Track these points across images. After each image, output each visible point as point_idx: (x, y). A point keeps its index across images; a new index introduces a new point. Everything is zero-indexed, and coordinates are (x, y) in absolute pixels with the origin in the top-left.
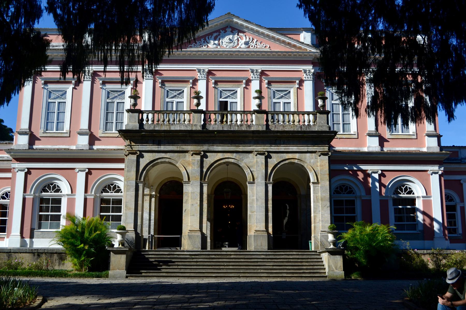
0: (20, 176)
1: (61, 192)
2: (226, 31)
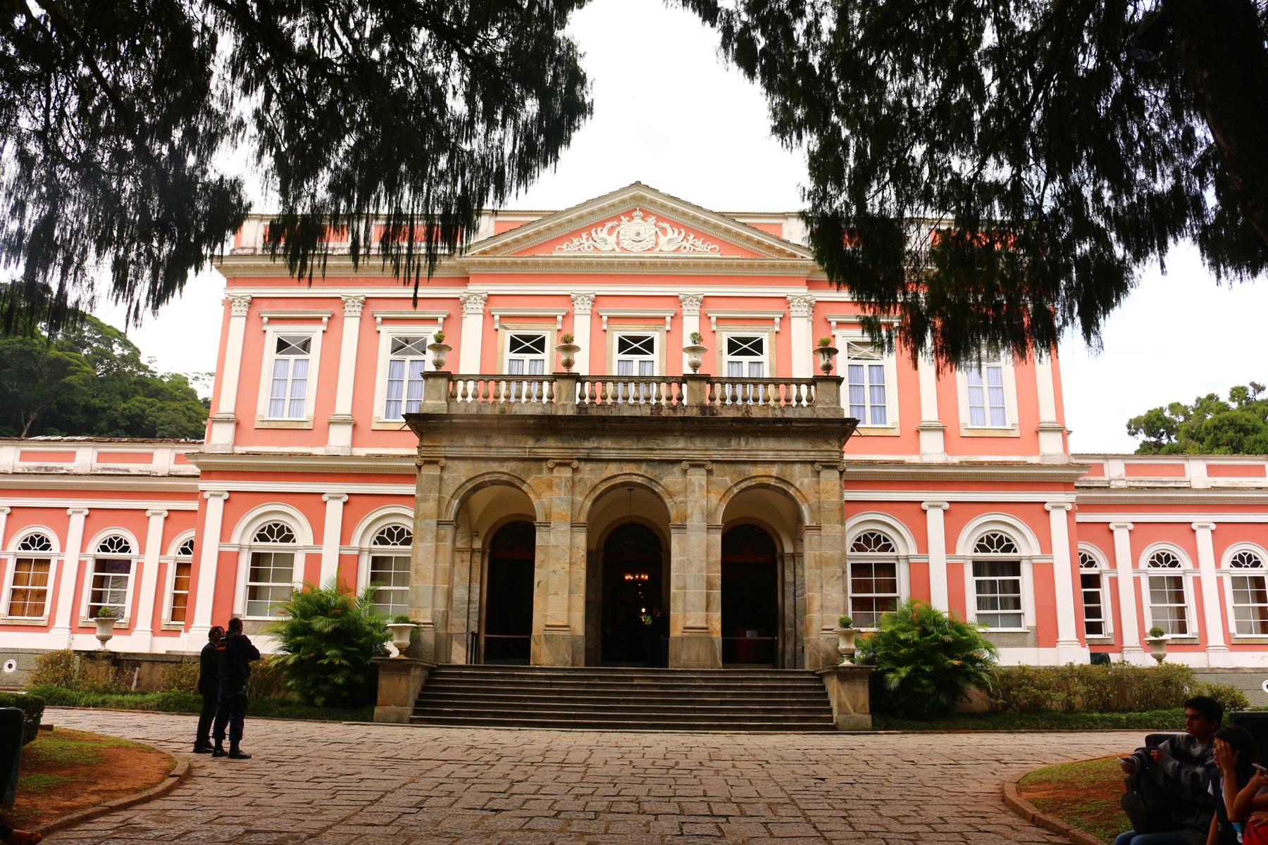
0: (215, 509)
1: (294, 541)
2: (632, 218)
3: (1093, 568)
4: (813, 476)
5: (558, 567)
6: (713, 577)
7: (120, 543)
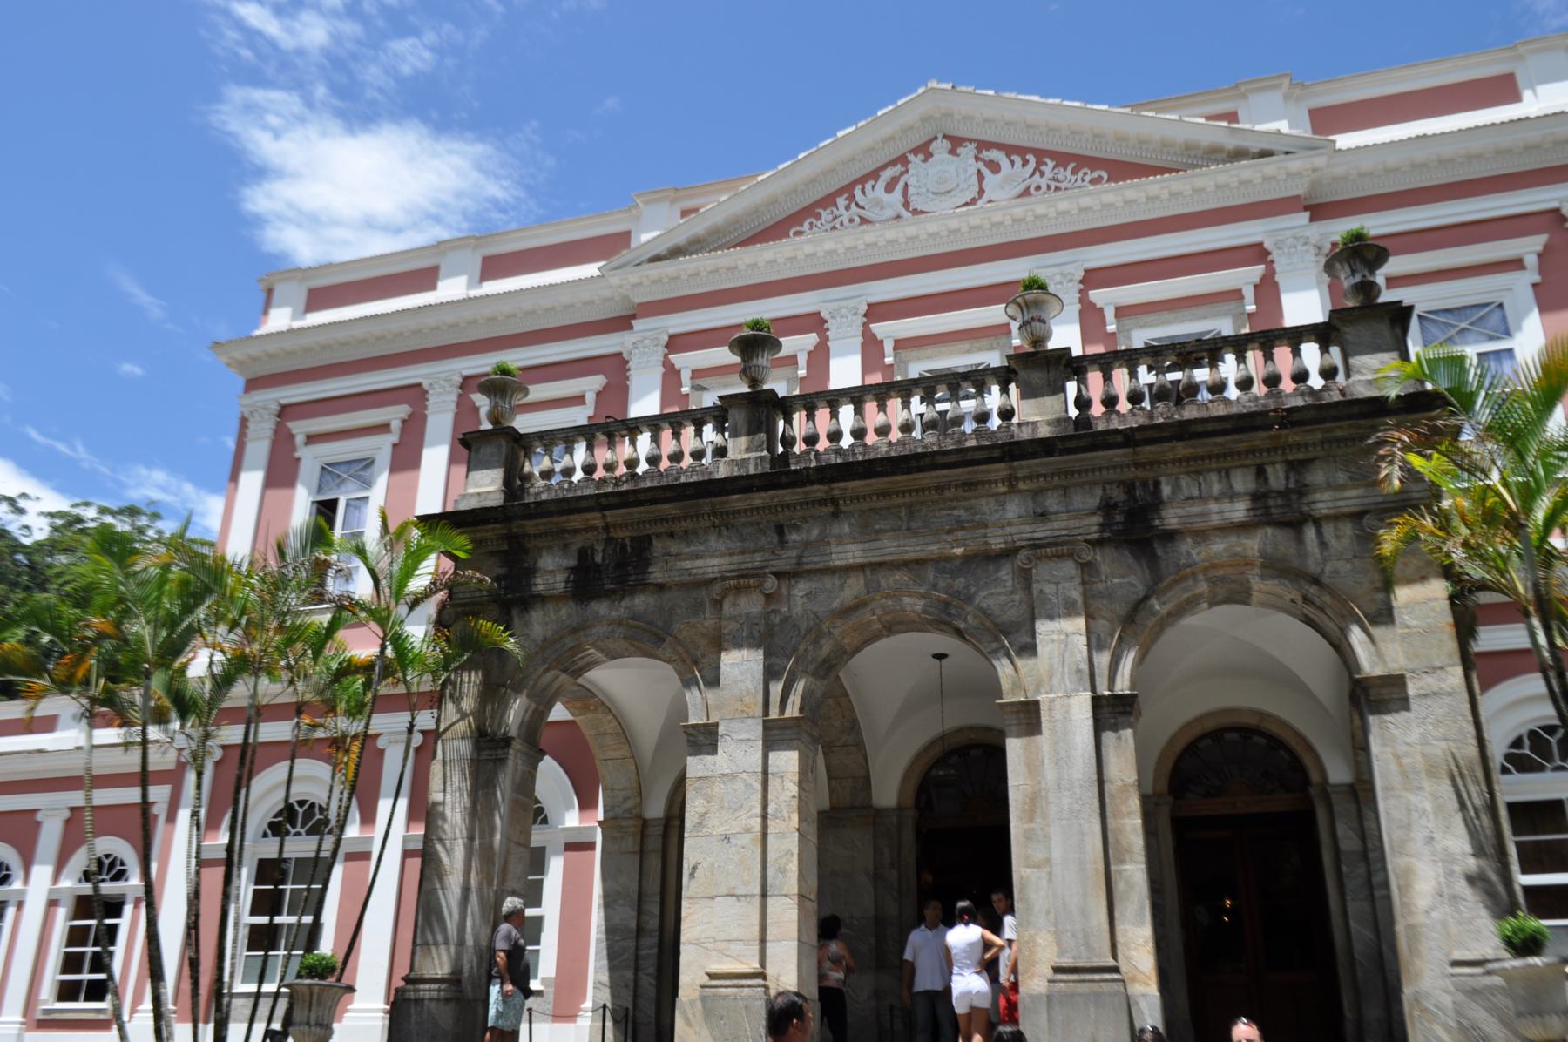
2: (928, 156)
7: (112, 865)
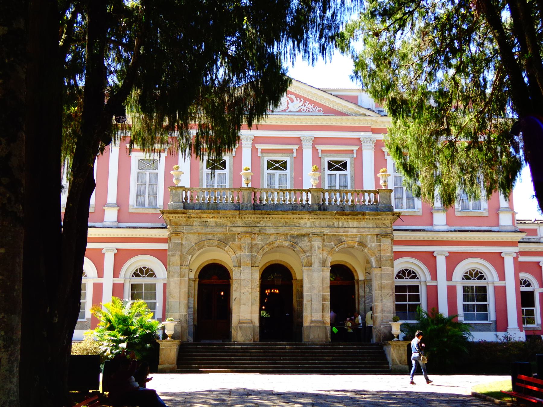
3: (530, 288)
4: (377, 242)
5: (245, 290)
6: (326, 295)
